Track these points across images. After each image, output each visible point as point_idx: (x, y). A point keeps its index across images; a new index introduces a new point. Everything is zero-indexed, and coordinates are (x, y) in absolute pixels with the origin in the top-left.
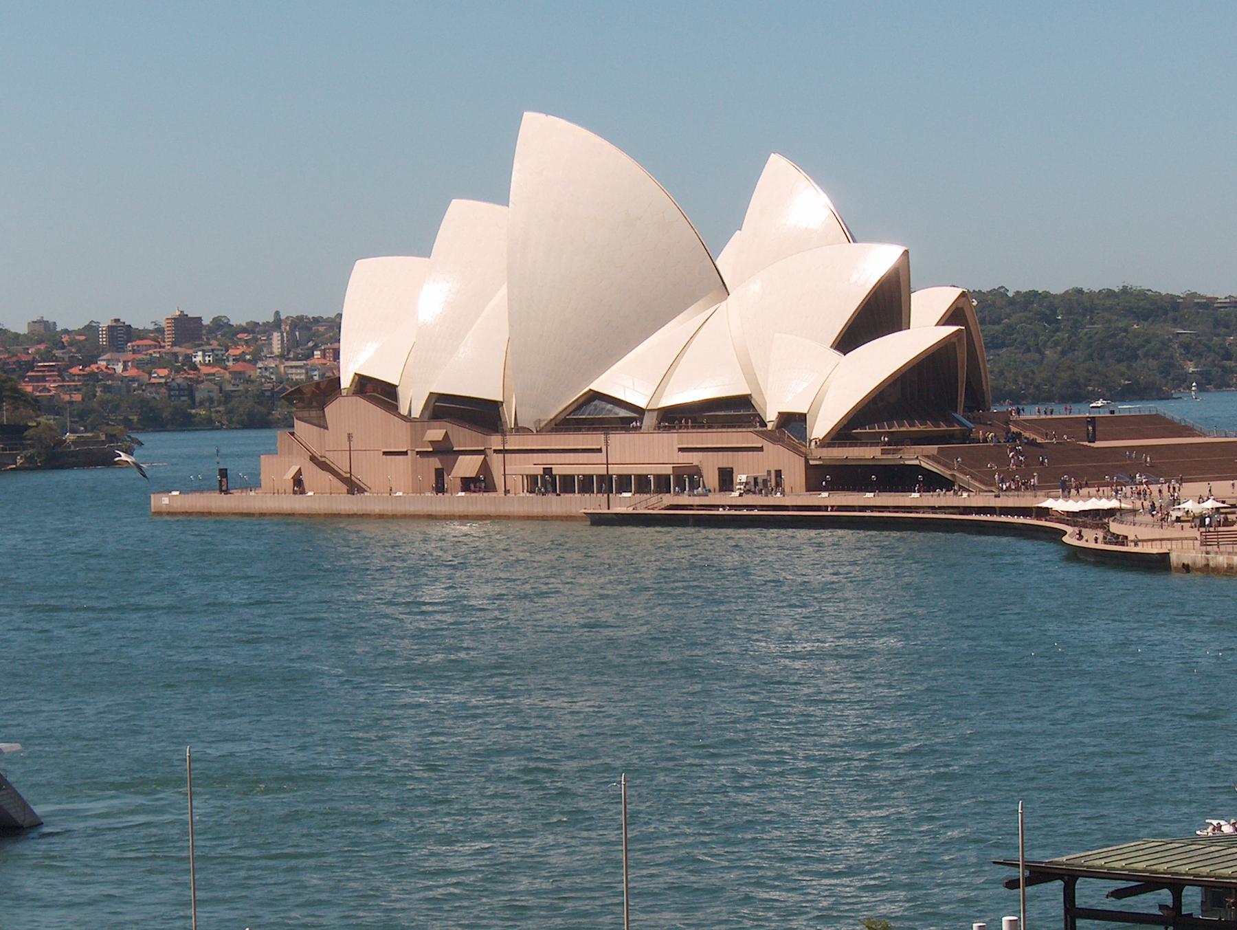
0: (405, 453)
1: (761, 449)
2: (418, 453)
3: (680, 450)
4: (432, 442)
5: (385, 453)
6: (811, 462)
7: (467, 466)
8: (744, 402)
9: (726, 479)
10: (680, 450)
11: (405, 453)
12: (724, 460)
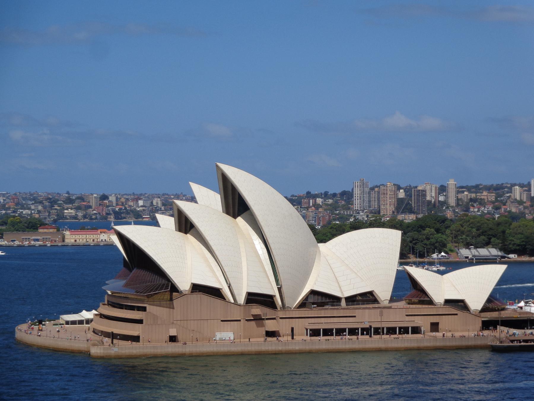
0: (240, 321)
1: (456, 314)
2: (246, 320)
3: (407, 315)
4: (253, 316)
5: (222, 321)
6: (483, 319)
7: (270, 325)
8: (371, 293)
9: (435, 327)
10: (407, 315)
11: (240, 321)
12: (435, 319)
